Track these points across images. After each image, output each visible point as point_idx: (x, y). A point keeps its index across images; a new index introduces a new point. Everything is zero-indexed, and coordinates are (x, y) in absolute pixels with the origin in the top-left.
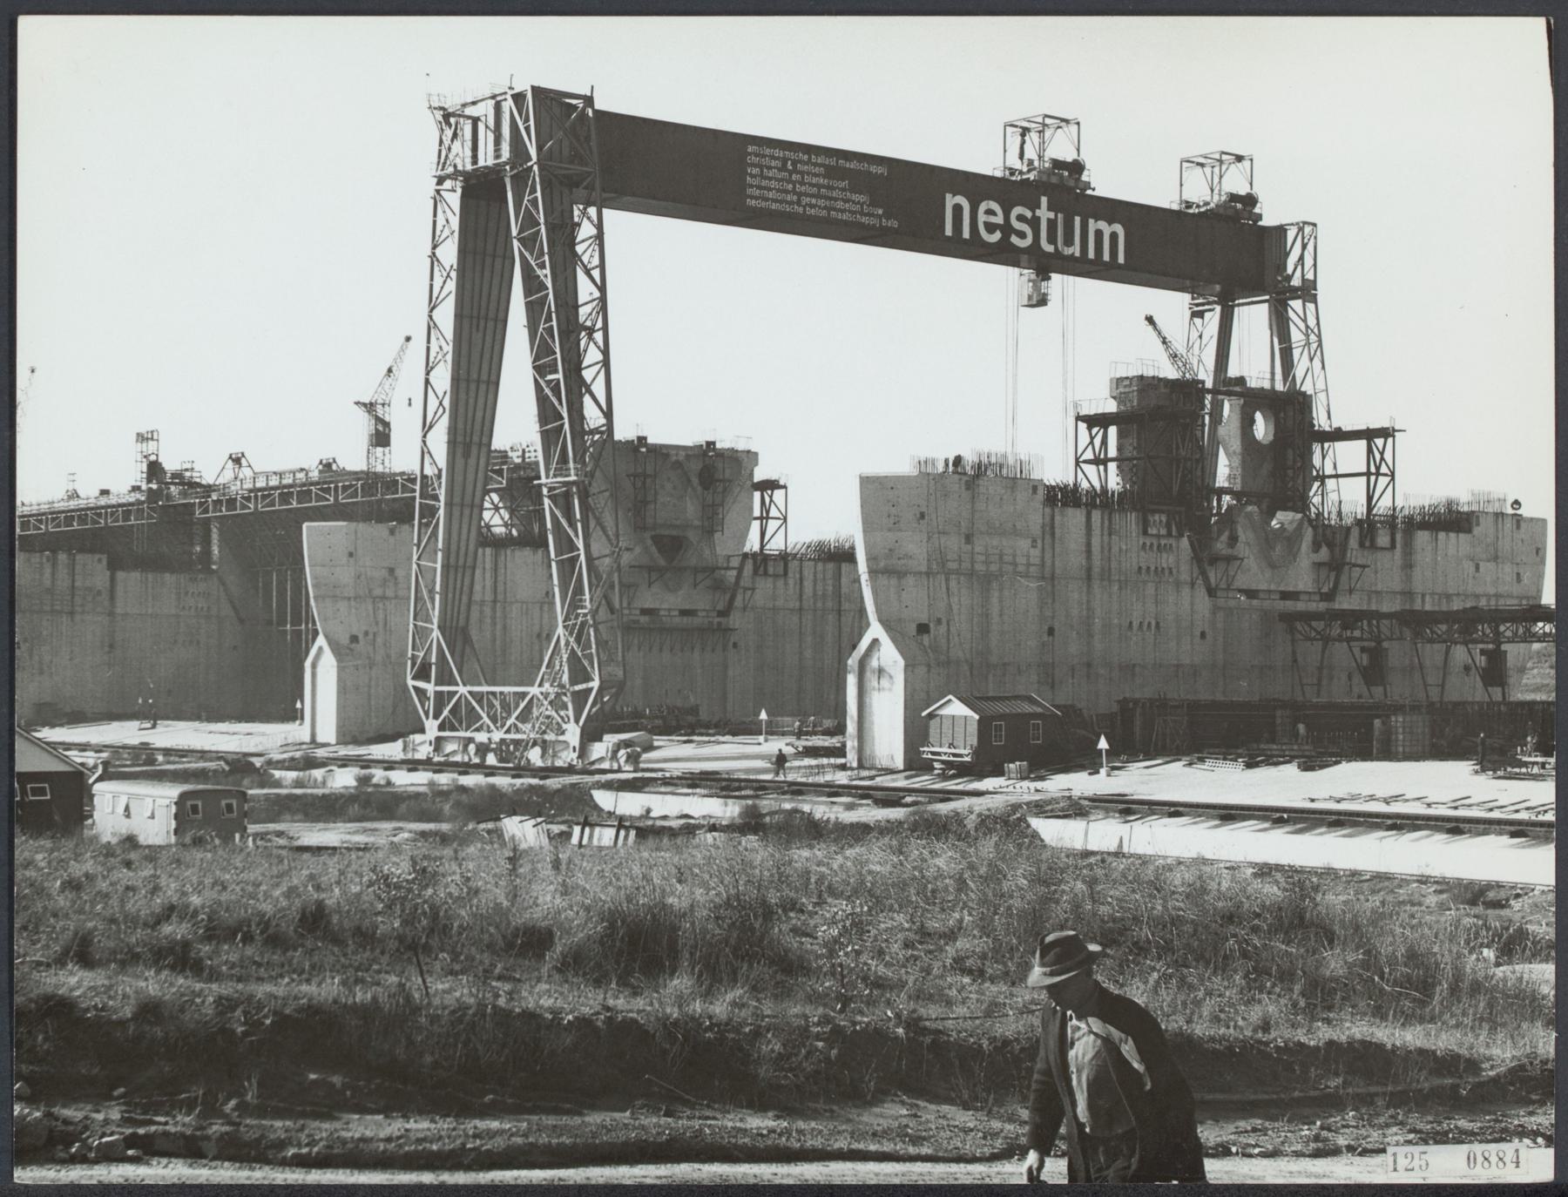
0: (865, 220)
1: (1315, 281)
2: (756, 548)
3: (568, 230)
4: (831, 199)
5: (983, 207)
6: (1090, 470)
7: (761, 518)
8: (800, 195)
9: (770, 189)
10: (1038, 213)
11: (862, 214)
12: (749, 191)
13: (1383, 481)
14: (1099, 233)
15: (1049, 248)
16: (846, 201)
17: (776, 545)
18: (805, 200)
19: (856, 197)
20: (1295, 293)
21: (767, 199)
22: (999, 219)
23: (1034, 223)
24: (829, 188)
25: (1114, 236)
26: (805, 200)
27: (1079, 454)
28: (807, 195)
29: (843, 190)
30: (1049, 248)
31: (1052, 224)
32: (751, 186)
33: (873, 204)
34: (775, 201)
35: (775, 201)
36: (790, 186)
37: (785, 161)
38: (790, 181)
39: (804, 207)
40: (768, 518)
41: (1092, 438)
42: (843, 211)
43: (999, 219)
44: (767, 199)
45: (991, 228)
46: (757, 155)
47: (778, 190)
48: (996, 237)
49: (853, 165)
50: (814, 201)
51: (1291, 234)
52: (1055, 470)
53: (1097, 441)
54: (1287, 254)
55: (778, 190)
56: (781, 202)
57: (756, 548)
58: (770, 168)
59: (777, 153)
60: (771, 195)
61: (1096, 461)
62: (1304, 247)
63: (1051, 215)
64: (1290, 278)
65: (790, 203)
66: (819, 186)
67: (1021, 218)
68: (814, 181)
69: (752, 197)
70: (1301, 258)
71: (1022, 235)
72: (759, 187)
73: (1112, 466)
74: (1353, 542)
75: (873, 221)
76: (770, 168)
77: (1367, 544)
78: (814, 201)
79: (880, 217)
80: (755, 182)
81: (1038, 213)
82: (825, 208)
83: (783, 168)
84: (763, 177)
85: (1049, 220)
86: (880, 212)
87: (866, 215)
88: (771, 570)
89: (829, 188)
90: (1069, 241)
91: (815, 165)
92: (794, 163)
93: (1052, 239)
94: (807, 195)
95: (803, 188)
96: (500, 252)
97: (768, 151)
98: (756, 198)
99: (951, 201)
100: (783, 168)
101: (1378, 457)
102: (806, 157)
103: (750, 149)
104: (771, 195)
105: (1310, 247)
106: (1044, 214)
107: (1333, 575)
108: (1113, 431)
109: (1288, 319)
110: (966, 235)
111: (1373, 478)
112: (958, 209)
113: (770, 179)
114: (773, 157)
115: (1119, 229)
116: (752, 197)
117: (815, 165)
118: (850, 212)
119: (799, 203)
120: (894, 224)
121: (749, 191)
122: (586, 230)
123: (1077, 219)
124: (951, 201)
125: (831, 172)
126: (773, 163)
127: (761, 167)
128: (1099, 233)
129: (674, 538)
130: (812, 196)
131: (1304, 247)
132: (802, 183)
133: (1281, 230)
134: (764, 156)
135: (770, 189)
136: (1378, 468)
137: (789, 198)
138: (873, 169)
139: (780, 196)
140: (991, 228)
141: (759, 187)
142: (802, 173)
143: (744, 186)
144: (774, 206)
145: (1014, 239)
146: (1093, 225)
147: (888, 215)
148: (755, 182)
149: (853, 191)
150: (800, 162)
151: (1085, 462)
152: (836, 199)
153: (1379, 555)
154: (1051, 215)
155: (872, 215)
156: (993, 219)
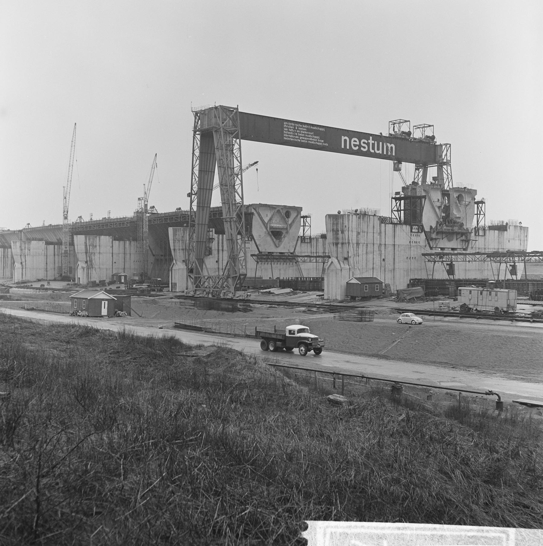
0: (318, 144)
1: (450, 160)
2: (302, 235)
3: (231, 146)
4: (308, 137)
5: (353, 140)
6: (396, 213)
7: (303, 226)
8: (299, 136)
9: (291, 135)
10: (369, 141)
11: (318, 142)
13: (482, 216)
14: (387, 147)
16: (313, 138)
17: (307, 234)
18: (301, 138)
19: (315, 137)
20: (445, 164)
21: (290, 138)
22: (358, 143)
23: (368, 144)
24: (308, 134)
25: (392, 148)
26: (301, 138)
27: (392, 208)
28: (301, 136)
29: (312, 135)
30: (373, 151)
31: (373, 144)
32: (285, 134)
33: (321, 139)
34: (292, 138)
35: (292, 138)
36: (297, 134)
37: (295, 126)
38: (297, 132)
40: (305, 226)
41: (396, 204)
43: (358, 143)
44: (290, 138)
45: (355, 146)
47: (293, 135)
48: (357, 148)
49: (315, 128)
50: (303, 138)
51: (444, 147)
52: (386, 213)
53: (398, 205)
54: (443, 152)
56: (294, 138)
57: (302, 235)
59: (293, 124)
61: (398, 211)
62: (447, 151)
63: (373, 142)
64: (443, 159)
65: (297, 139)
66: (305, 134)
67: (364, 143)
68: (304, 132)
69: (285, 137)
70: (446, 154)
71: (364, 148)
72: (288, 134)
73: (402, 212)
74: (473, 234)
75: (320, 144)
77: (477, 234)
78: (303, 138)
79: (323, 143)
80: (286, 132)
81: (369, 141)
82: (307, 140)
83: (294, 129)
86: (323, 141)
88: (306, 241)
89: (308, 134)
90: (378, 149)
91: (304, 128)
92: (298, 127)
93: (373, 149)
94: (301, 136)
96: (212, 153)
97: (290, 124)
98: (287, 137)
99: (343, 138)
101: (480, 209)
102: (301, 126)
105: (449, 150)
106: (371, 141)
107: (467, 243)
108: (402, 202)
109: (443, 171)
110: (348, 148)
111: (479, 215)
112: (345, 140)
113: (291, 132)
114: (291, 126)
115: (393, 145)
116: (285, 137)
117: (304, 128)
121: (285, 135)
122: (236, 146)
123: (381, 143)
124: (343, 138)
125: (308, 130)
127: (288, 128)
129: (278, 232)
130: (303, 137)
131: (447, 151)
132: (300, 133)
133: (441, 145)
134: (289, 125)
135: (291, 135)
136: (480, 212)
138: (321, 129)
140: (355, 146)
141: (288, 134)
142: (300, 130)
143: (283, 133)
145: (362, 149)
147: (325, 142)
148: (286, 132)
150: (300, 127)
151: (394, 211)
152: (310, 138)
153: (480, 237)
154: (373, 142)
155: (320, 142)
156: (355, 143)
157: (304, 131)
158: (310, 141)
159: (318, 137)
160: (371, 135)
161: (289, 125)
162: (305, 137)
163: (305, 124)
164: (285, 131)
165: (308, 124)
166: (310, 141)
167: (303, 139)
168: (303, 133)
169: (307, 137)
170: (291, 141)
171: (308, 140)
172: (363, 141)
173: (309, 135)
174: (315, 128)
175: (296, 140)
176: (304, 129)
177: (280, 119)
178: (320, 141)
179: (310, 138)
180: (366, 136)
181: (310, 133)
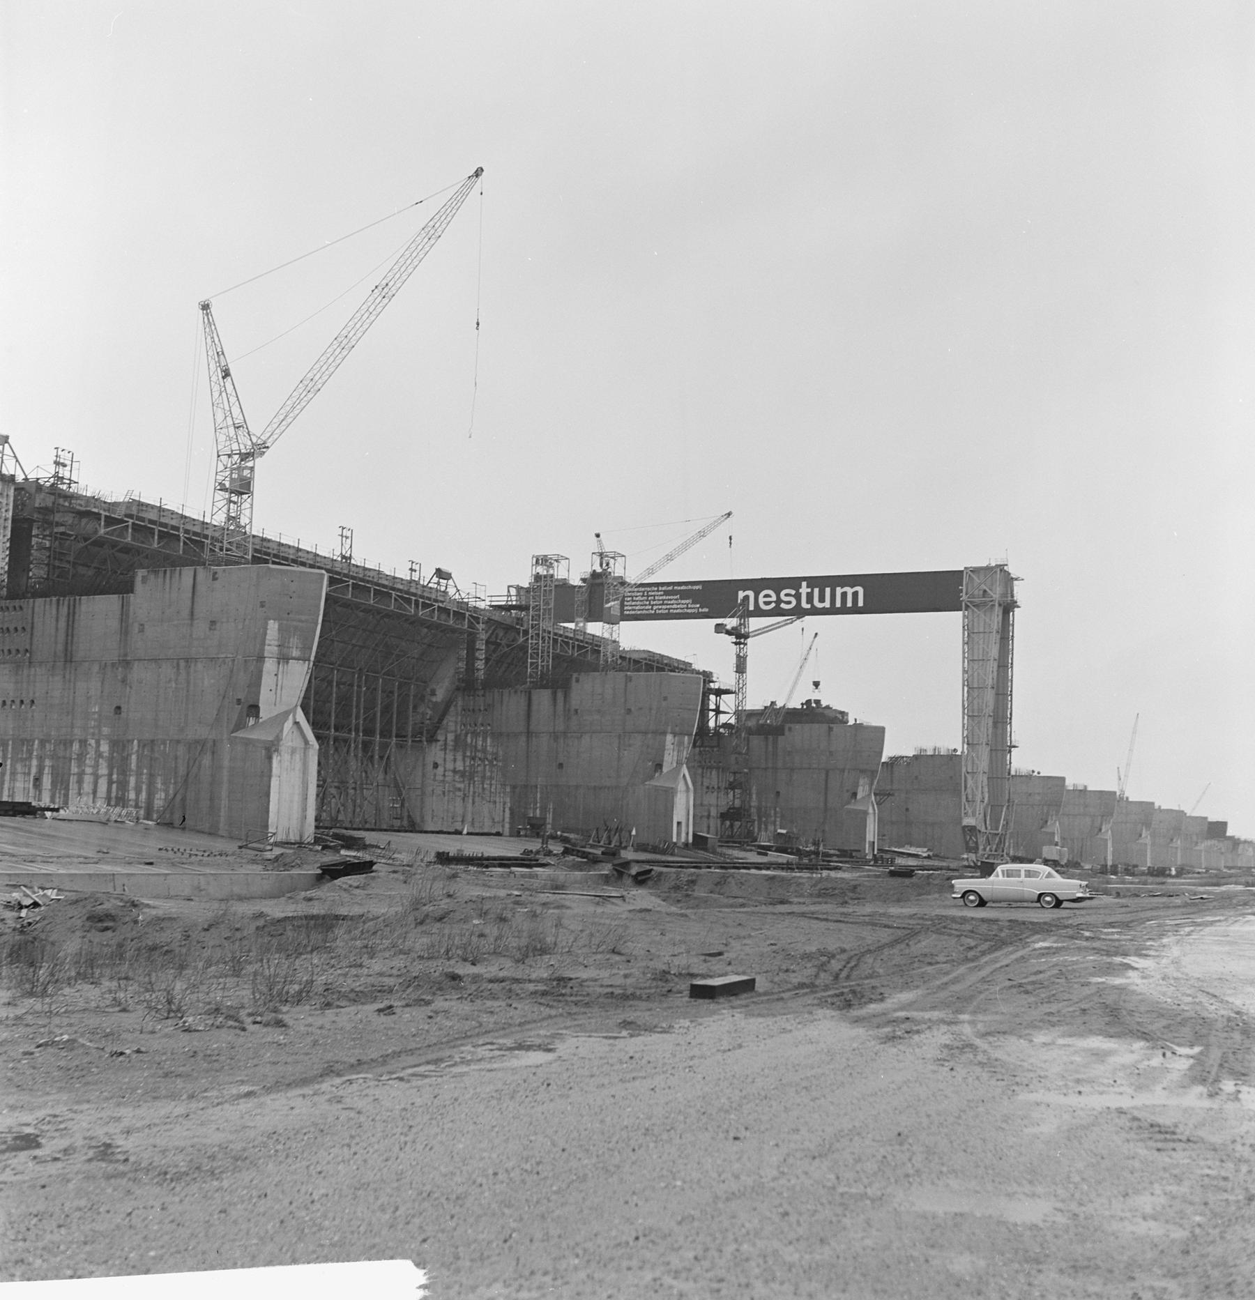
0: (689, 611)
14: (844, 595)
15: (809, 606)
18: (655, 608)
19: (683, 602)
25: (855, 594)
26: (655, 608)
31: (810, 598)
43: (774, 598)
45: (767, 603)
48: (773, 605)
63: (809, 590)
66: (663, 600)
71: (789, 603)
75: (693, 611)
85: (808, 593)
90: (822, 600)
99: (741, 594)
115: (860, 590)
123: (828, 590)
124: (741, 594)
125: (666, 593)
128: (844, 595)
140: (767, 603)
145: (783, 605)
146: (839, 591)
149: (681, 599)
154: (809, 590)
159: (687, 601)
160: (804, 579)
162: (663, 604)
163: (663, 584)
172: (787, 591)
175: (644, 612)
180: (794, 583)
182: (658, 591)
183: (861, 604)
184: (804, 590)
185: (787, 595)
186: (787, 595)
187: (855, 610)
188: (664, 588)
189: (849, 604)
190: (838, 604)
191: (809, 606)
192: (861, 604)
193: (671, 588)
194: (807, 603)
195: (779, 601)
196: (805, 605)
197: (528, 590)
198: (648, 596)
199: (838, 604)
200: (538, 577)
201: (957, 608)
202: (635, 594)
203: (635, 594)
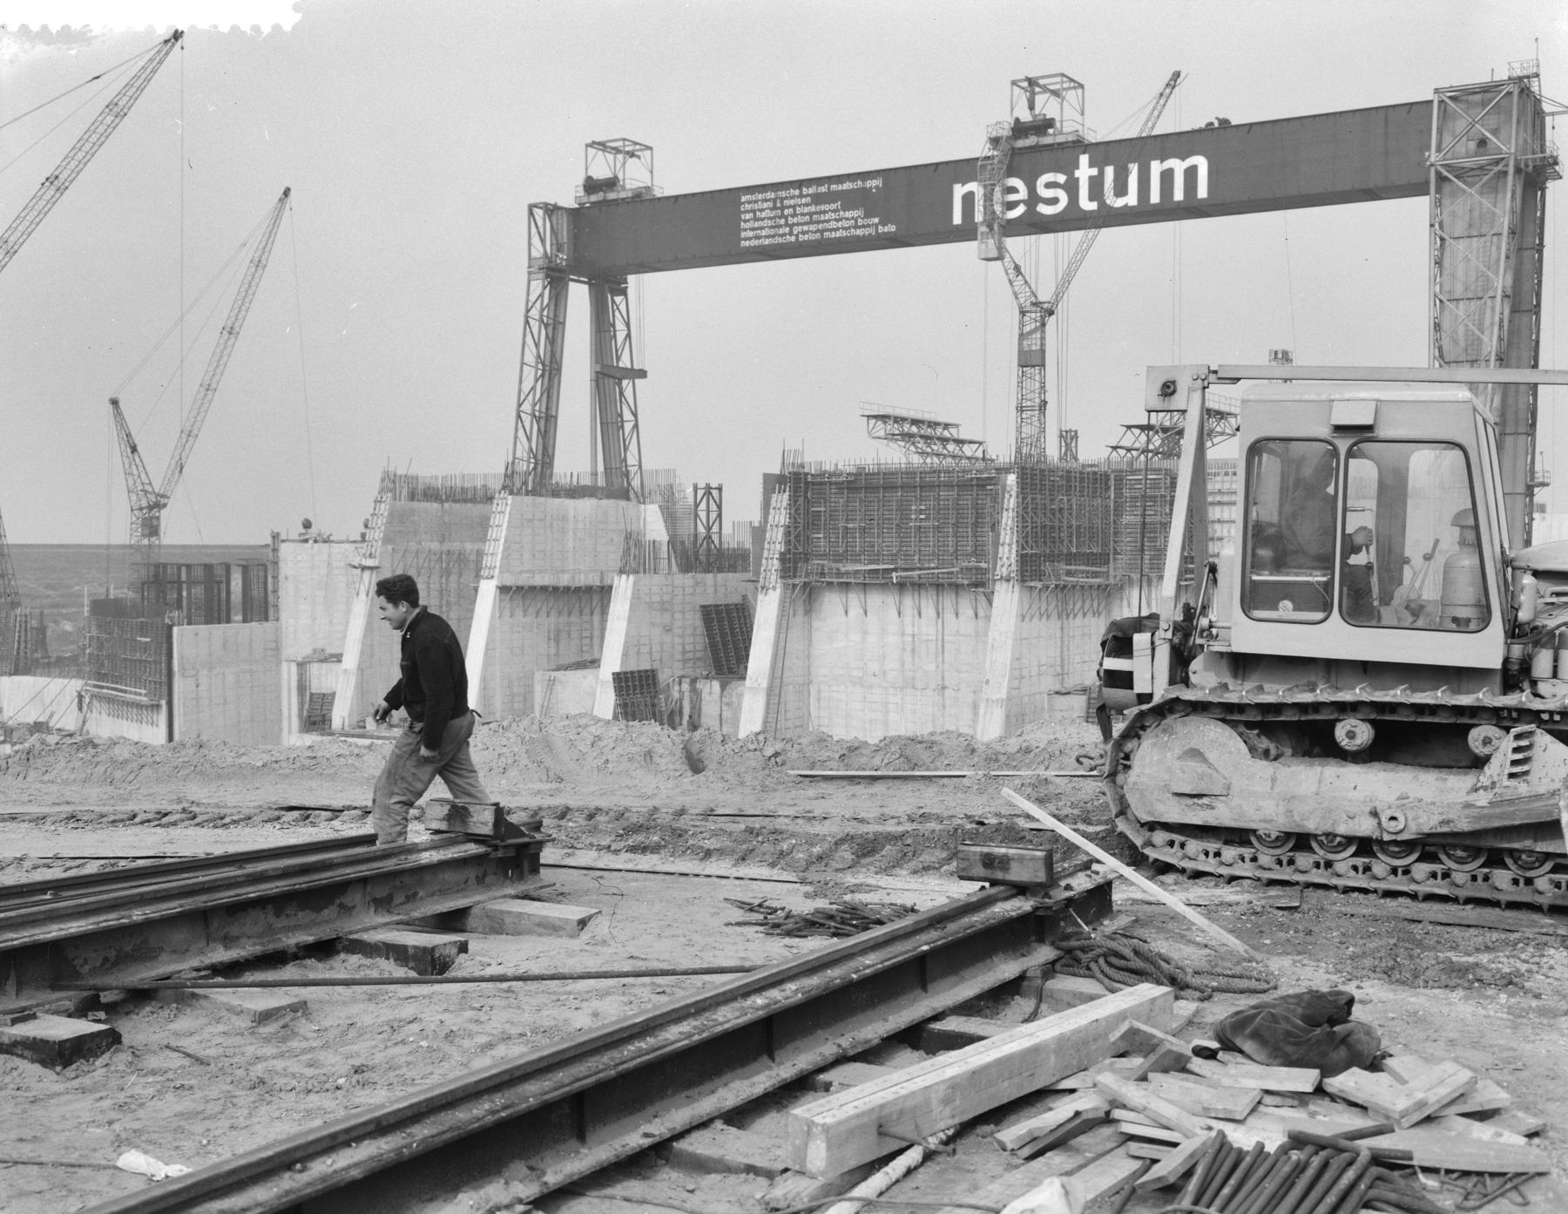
0: (859, 232)
9: (762, 228)
11: (856, 227)
12: (743, 234)
14: (1167, 176)
15: (1093, 206)
18: (796, 230)
19: (848, 214)
25: (1191, 173)
26: (796, 230)
28: (798, 224)
29: (835, 211)
31: (1096, 185)
32: (745, 230)
33: (867, 215)
38: (783, 216)
39: (797, 236)
42: (838, 229)
43: (1023, 194)
46: (749, 202)
47: (772, 227)
48: (1021, 210)
49: (847, 186)
50: (806, 228)
55: (772, 227)
56: (773, 236)
58: (762, 210)
60: (764, 233)
63: (1094, 172)
65: (784, 235)
66: (811, 214)
68: (806, 210)
69: (745, 239)
71: (1054, 201)
72: (752, 229)
75: (867, 231)
76: (762, 210)
78: (806, 228)
79: (876, 225)
82: (818, 231)
84: (756, 219)
87: (860, 227)
90: (1121, 190)
94: (798, 224)
95: (795, 220)
97: (760, 196)
98: (750, 239)
99: (959, 191)
100: (775, 208)
102: (797, 192)
103: (743, 199)
104: (764, 233)
112: (968, 199)
113: (763, 219)
114: (766, 200)
115: (1201, 163)
116: (745, 239)
118: (844, 228)
119: (791, 234)
120: (891, 228)
121: (743, 234)
123: (1134, 169)
124: (959, 191)
125: (817, 199)
126: (765, 205)
127: (754, 211)
128: (1167, 176)
132: (794, 215)
134: (756, 202)
135: (762, 228)
137: (781, 231)
139: (772, 232)
141: (752, 229)
142: (794, 207)
143: (739, 230)
144: (767, 242)
145: (1044, 209)
146: (1156, 168)
152: (828, 221)
154: (1094, 172)
155: (868, 226)
156: (1012, 197)
157: (806, 205)
158: (831, 230)
159: (855, 213)
161: (756, 202)
164: (745, 221)
165: (819, 181)
166: (831, 230)
167: (804, 233)
168: (803, 215)
169: (818, 222)
170: (763, 246)
171: (822, 232)
173: (825, 212)
174: (847, 186)
175: (779, 240)
176: (791, 197)
177: (730, 190)
178: (866, 222)
179: (828, 221)
181: (823, 207)
182: (801, 196)
183: (1202, 192)
184: (1085, 171)
185: (1049, 185)
186: (1049, 185)
187: (1192, 209)
188: (811, 191)
189: (1179, 195)
190: (1155, 197)
191: (1093, 206)
192: (1202, 192)
193: (823, 189)
194: (1091, 199)
195: (1033, 199)
196: (1087, 205)
197: (576, 214)
198: (783, 208)
199: (1155, 197)
200: (591, 186)
201: (1419, 189)
202: (760, 205)
203: (760, 205)
